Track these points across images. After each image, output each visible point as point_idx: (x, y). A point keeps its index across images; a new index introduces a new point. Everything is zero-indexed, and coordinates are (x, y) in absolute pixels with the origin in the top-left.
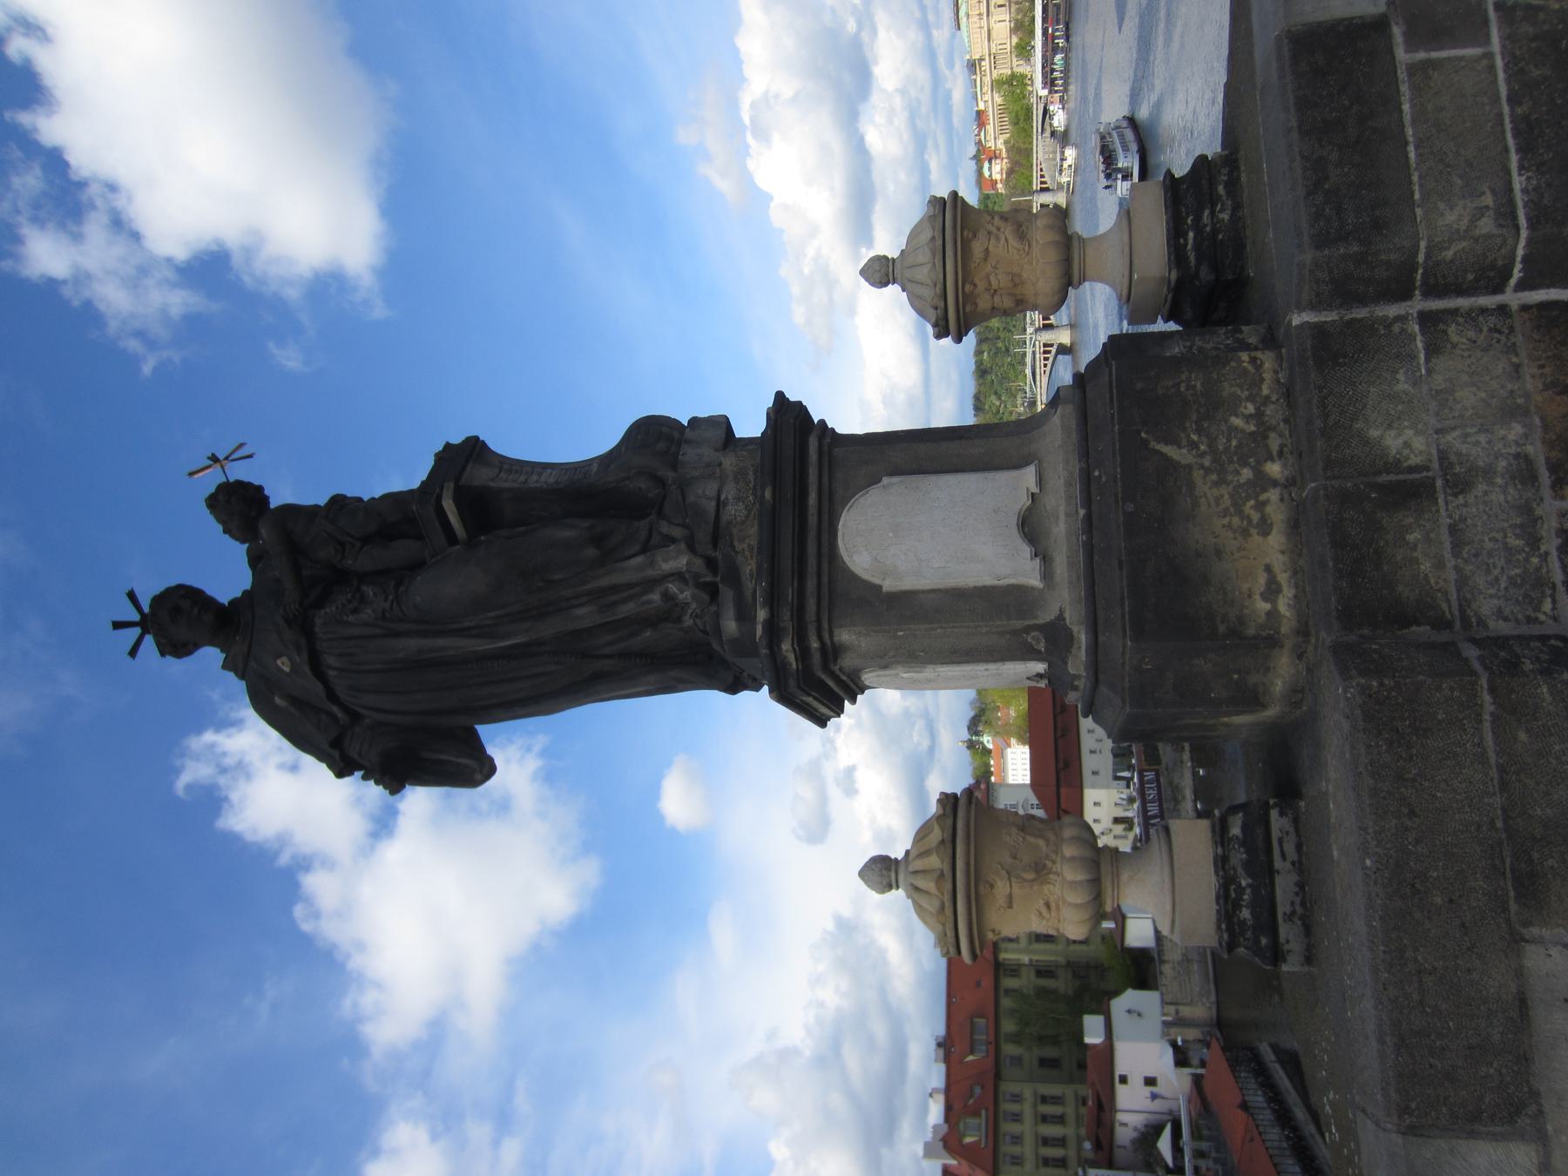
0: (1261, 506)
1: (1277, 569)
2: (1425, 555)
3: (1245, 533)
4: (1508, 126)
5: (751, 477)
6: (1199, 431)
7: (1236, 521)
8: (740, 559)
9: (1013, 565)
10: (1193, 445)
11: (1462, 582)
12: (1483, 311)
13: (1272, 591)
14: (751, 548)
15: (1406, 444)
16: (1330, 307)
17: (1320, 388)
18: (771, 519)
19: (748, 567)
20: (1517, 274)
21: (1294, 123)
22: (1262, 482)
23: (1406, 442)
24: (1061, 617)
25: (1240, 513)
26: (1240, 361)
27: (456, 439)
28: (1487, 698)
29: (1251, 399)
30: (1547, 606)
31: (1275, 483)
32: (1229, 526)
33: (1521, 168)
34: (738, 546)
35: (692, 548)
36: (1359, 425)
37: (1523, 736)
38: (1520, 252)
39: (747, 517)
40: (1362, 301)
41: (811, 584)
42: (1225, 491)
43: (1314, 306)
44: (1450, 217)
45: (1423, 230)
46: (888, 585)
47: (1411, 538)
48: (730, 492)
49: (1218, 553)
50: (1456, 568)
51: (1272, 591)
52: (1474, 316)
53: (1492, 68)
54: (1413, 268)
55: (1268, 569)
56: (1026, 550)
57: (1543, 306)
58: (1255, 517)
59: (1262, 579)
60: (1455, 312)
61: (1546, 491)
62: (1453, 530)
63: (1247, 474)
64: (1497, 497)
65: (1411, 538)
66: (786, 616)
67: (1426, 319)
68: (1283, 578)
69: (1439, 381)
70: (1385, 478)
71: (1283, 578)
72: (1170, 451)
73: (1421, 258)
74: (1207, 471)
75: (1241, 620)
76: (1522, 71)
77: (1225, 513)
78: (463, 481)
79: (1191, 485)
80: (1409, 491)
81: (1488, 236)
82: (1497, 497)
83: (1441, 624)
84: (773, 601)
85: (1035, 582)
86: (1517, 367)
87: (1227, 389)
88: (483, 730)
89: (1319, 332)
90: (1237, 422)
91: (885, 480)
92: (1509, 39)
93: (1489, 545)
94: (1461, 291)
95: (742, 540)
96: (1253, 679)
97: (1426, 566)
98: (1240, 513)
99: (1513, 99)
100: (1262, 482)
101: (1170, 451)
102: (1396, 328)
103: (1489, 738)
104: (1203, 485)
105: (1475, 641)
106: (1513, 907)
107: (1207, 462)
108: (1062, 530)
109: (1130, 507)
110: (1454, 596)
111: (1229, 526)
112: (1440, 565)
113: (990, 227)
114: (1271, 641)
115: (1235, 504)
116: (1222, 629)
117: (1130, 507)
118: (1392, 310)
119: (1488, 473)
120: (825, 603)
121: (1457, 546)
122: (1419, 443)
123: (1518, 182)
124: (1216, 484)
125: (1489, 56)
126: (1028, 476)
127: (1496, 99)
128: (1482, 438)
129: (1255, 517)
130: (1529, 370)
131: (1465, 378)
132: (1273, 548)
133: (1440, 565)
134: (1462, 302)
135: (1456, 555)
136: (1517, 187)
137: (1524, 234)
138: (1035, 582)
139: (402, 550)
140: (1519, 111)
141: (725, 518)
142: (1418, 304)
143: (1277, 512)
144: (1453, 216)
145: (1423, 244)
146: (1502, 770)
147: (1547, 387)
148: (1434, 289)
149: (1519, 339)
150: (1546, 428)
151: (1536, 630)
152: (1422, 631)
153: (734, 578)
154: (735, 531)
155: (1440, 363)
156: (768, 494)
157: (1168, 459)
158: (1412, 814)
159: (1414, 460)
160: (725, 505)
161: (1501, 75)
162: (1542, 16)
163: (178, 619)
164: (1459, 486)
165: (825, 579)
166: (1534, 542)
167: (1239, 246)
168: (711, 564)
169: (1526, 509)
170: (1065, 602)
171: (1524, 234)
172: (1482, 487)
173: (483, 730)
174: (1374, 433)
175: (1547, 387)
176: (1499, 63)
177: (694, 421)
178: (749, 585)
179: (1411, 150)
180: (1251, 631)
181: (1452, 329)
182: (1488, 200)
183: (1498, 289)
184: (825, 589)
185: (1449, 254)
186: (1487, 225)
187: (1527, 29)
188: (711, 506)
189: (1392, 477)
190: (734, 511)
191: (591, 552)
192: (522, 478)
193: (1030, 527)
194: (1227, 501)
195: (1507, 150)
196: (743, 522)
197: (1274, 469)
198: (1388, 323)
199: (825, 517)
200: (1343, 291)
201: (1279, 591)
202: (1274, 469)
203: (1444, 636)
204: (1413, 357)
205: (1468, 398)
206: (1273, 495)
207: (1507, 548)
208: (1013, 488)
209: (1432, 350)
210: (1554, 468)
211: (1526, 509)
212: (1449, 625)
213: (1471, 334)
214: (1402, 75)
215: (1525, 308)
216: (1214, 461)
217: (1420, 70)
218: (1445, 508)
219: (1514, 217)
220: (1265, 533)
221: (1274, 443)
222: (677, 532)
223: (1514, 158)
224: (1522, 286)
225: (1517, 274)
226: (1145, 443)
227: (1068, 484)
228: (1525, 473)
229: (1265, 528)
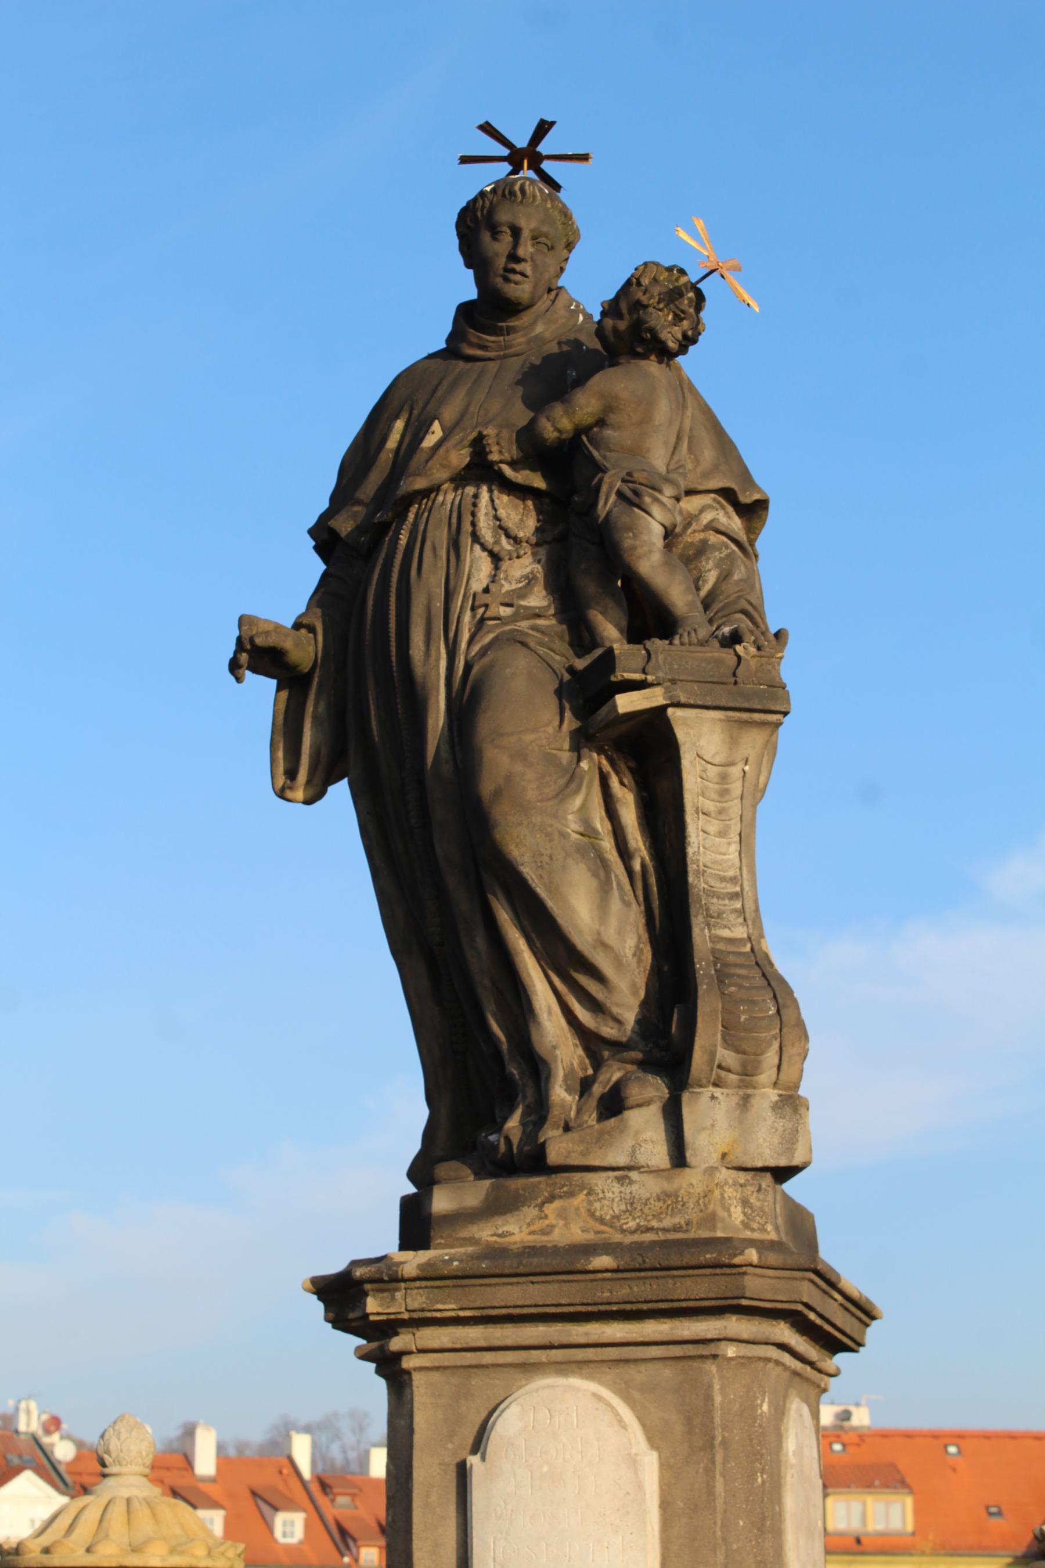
5: (667, 1222)
8: (530, 1212)
14: (544, 1232)
18: (564, 1263)
19: (515, 1230)
34: (550, 1209)
39: (601, 1221)
41: (474, 1335)
48: (644, 1187)
95: (562, 1215)
141: (598, 1180)
153: (496, 1207)
154: (579, 1200)
160: (619, 1179)
163: (499, 234)
165: (488, 1358)
178: (486, 1232)
184: (470, 1358)
196: (592, 1214)
199: (590, 1353)
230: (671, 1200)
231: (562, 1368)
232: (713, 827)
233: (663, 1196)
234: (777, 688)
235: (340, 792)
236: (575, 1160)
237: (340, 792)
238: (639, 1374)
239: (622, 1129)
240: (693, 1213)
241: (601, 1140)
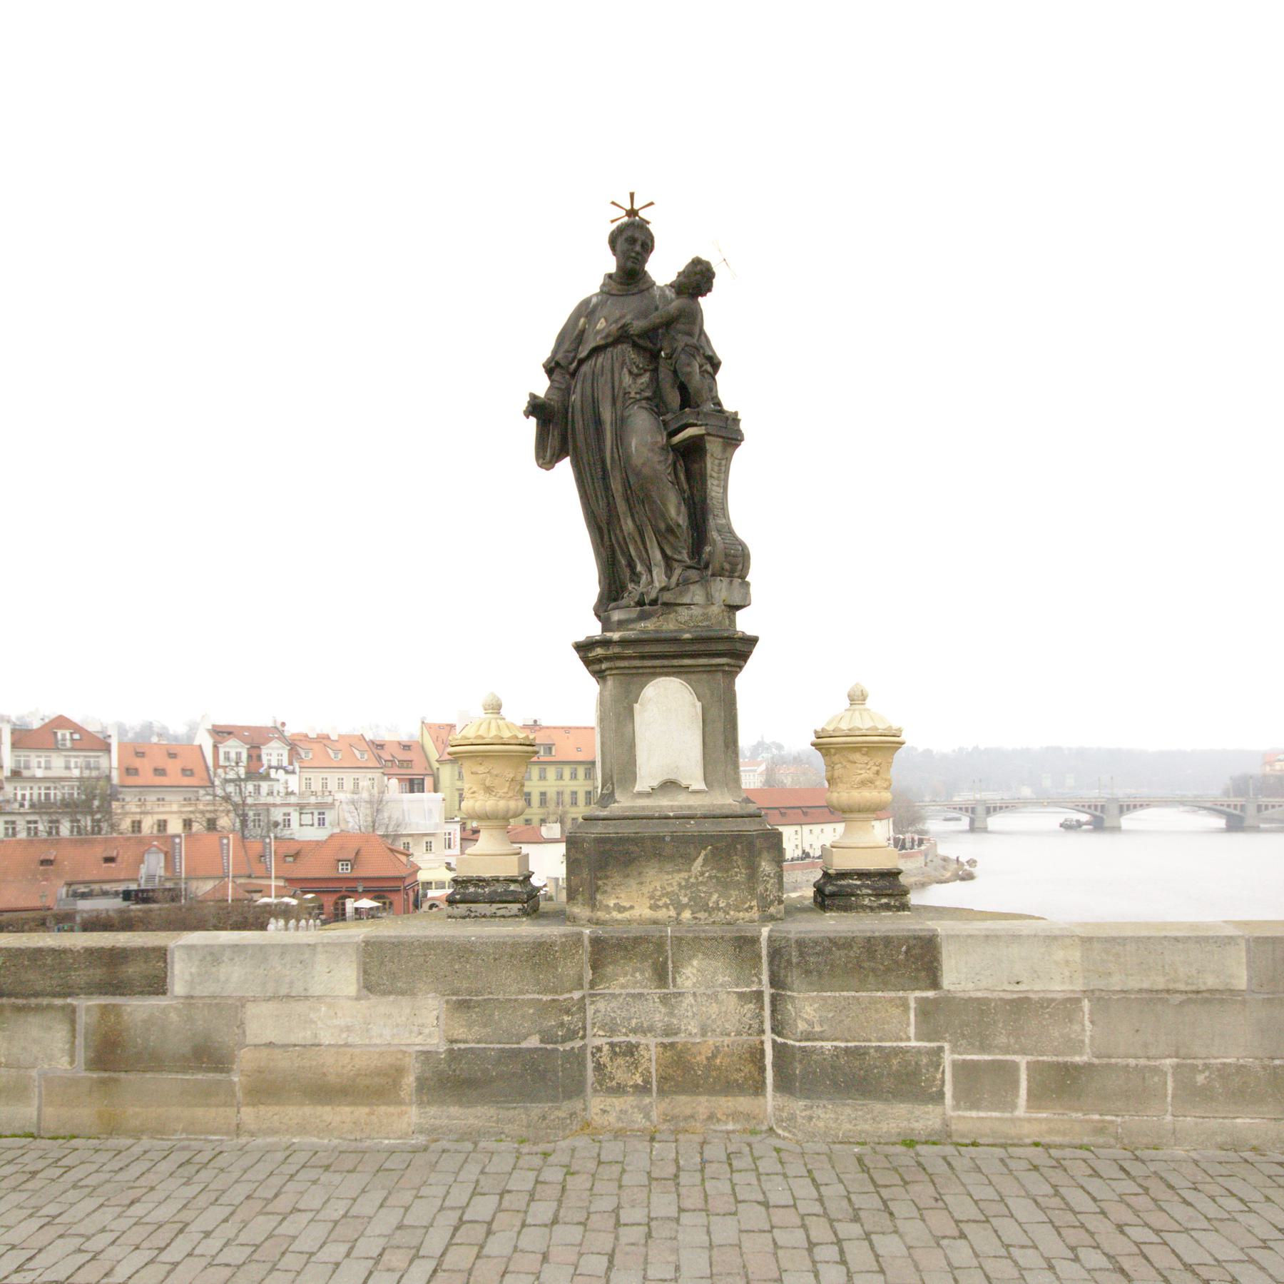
0: (666, 906)
1: (631, 912)
2: (627, 980)
3: (651, 898)
4: (863, 1044)
6: (710, 877)
7: (658, 893)
8: (655, 619)
9: (647, 778)
10: (702, 874)
11: (613, 996)
12: (762, 1022)
13: (621, 909)
15: (688, 978)
16: (769, 946)
17: (722, 938)
20: (779, 1040)
21: (877, 934)
22: (680, 908)
23: (690, 975)
24: (615, 801)
25: (663, 895)
26: (751, 900)
27: (742, 426)
28: (550, 997)
29: (728, 905)
30: (601, 1033)
31: (678, 914)
32: (656, 889)
33: (836, 1047)
35: (662, 589)
36: (700, 956)
37: (531, 1011)
38: (790, 1042)
40: (771, 963)
41: (637, 663)
42: (676, 888)
43: (770, 937)
44: (808, 1009)
45: (802, 995)
46: (636, 706)
47: (637, 974)
48: (696, 611)
49: (641, 883)
50: (620, 995)
51: (621, 909)
52: (759, 1017)
53: (901, 1040)
54: (784, 989)
55: (632, 907)
56: (655, 784)
57: (762, 1052)
58: (660, 903)
59: (627, 904)
60: (762, 1008)
61: (659, 1040)
62: (641, 995)
63: (685, 900)
64: (657, 1017)
65: (637, 974)
66: (617, 650)
67: (759, 995)
68: (626, 915)
69: (723, 996)
70: (670, 965)
71: (626, 915)
72: (700, 860)
73: (789, 993)
74: (687, 880)
75: (605, 892)
76: (897, 1055)
77: (663, 888)
78: (707, 438)
79: (680, 871)
80: (661, 976)
81: (797, 1027)
82: (657, 1017)
83: (593, 984)
84: (623, 642)
85: (638, 788)
86: (728, 1035)
87: (734, 893)
88: (567, 460)
89: (754, 941)
90: (715, 896)
91: (699, 704)
92: (919, 1051)
93: (633, 1010)
94: (773, 1011)
96: (579, 897)
97: (622, 980)
98: (663, 895)
99: (878, 1049)
100: (680, 908)
101: (700, 860)
102: (755, 979)
103: (531, 996)
104: (680, 877)
105: (583, 997)
106: (454, 998)
107: (692, 880)
108: (666, 803)
109: (668, 839)
110: (606, 991)
111: (656, 889)
112: (623, 986)
113: (871, 763)
114: (593, 907)
115: (668, 893)
116: (600, 883)
117: (668, 839)
118: (765, 978)
119: (671, 1014)
120: (626, 671)
121: (633, 996)
122: (688, 983)
123: (828, 1045)
124: (679, 884)
125: (908, 1039)
126: (700, 785)
127: (880, 1040)
128: (690, 1014)
129: (660, 903)
130: (727, 1040)
131: (724, 1009)
132: (642, 911)
133: (623, 986)
134: (767, 1012)
135: (628, 995)
136: (823, 1044)
137: (797, 1044)
138: (638, 788)
139: (674, 398)
140: (872, 1051)
141: (680, 609)
142: (768, 991)
143: (661, 914)
144: (809, 1011)
145: (795, 994)
146: (516, 1000)
147: (716, 1047)
148: (774, 999)
149: (745, 1037)
150: (694, 1044)
151: (589, 1027)
152: (588, 975)
153: (643, 617)
155: (733, 1000)
156: (687, 636)
157: (695, 860)
158: (495, 959)
159: (679, 980)
161: (895, 1044)
162: (931, 1070)
164: (664, 1000)
166: (634, 1031)
167: (846, 908)
168: (654, 602)
169: (651, 1029)
170: (623, 803)
171: (797, 1044)
172: (663, 1010)
173: (567, 460)
174: (695, 963)
175: (716, 1047)
176: (903, 1044)
177: (748, 584)
179: (853, 993)
180: (598, 897)
181: (752, 1006)
182: (818, 1029)
183: (773, 1030)
185: (789, 1007)
186: (802, 1026)
187: (925, 1060)
188: (686, 600)
189: (670, 969)
190: (684, 614)
191: (662, 526)
192: (715, 475)
193: (670, 785)
194: (669, 889)
195: (847, 1041)
197: (687, 915)
198: (758, 975)
200: (776, 953)
201: (620, 912)
202: (687, 915)
203: (587, 986)
204: (737, 986)
205: (714, 1009)
206: (673, 913)
207: (630, 1019)
208: (692, 773)
209: (741, 996)
210: (672, 1045)
211: (651, 1029)
212: (592, 988)
213: (749, 1015)
214: (901, 994)
215: (762, 1043)
216: (693, 884)
217: (904, 1005)
218: (654, 992)
219: (808, 1040)
220: (650, 908)
221: (702, 915)
222: (674, 579)
223: (843, 1045)
224: (774, 1042)
225: (779, 1040)
226: (705, 848)
227: (690, 807)
228: (669, 1031)
229: (654, 907)
230: (706, 617)
231: (667, 674)
232: (715, 482)
233: (703, 614)
234: (739, 432)
235: (565, 466)
236: (672, 601)
237: (565, 466)
238: (693, 677)
239: (688, 590)
240: (714, 621)
241: (681, 594)
